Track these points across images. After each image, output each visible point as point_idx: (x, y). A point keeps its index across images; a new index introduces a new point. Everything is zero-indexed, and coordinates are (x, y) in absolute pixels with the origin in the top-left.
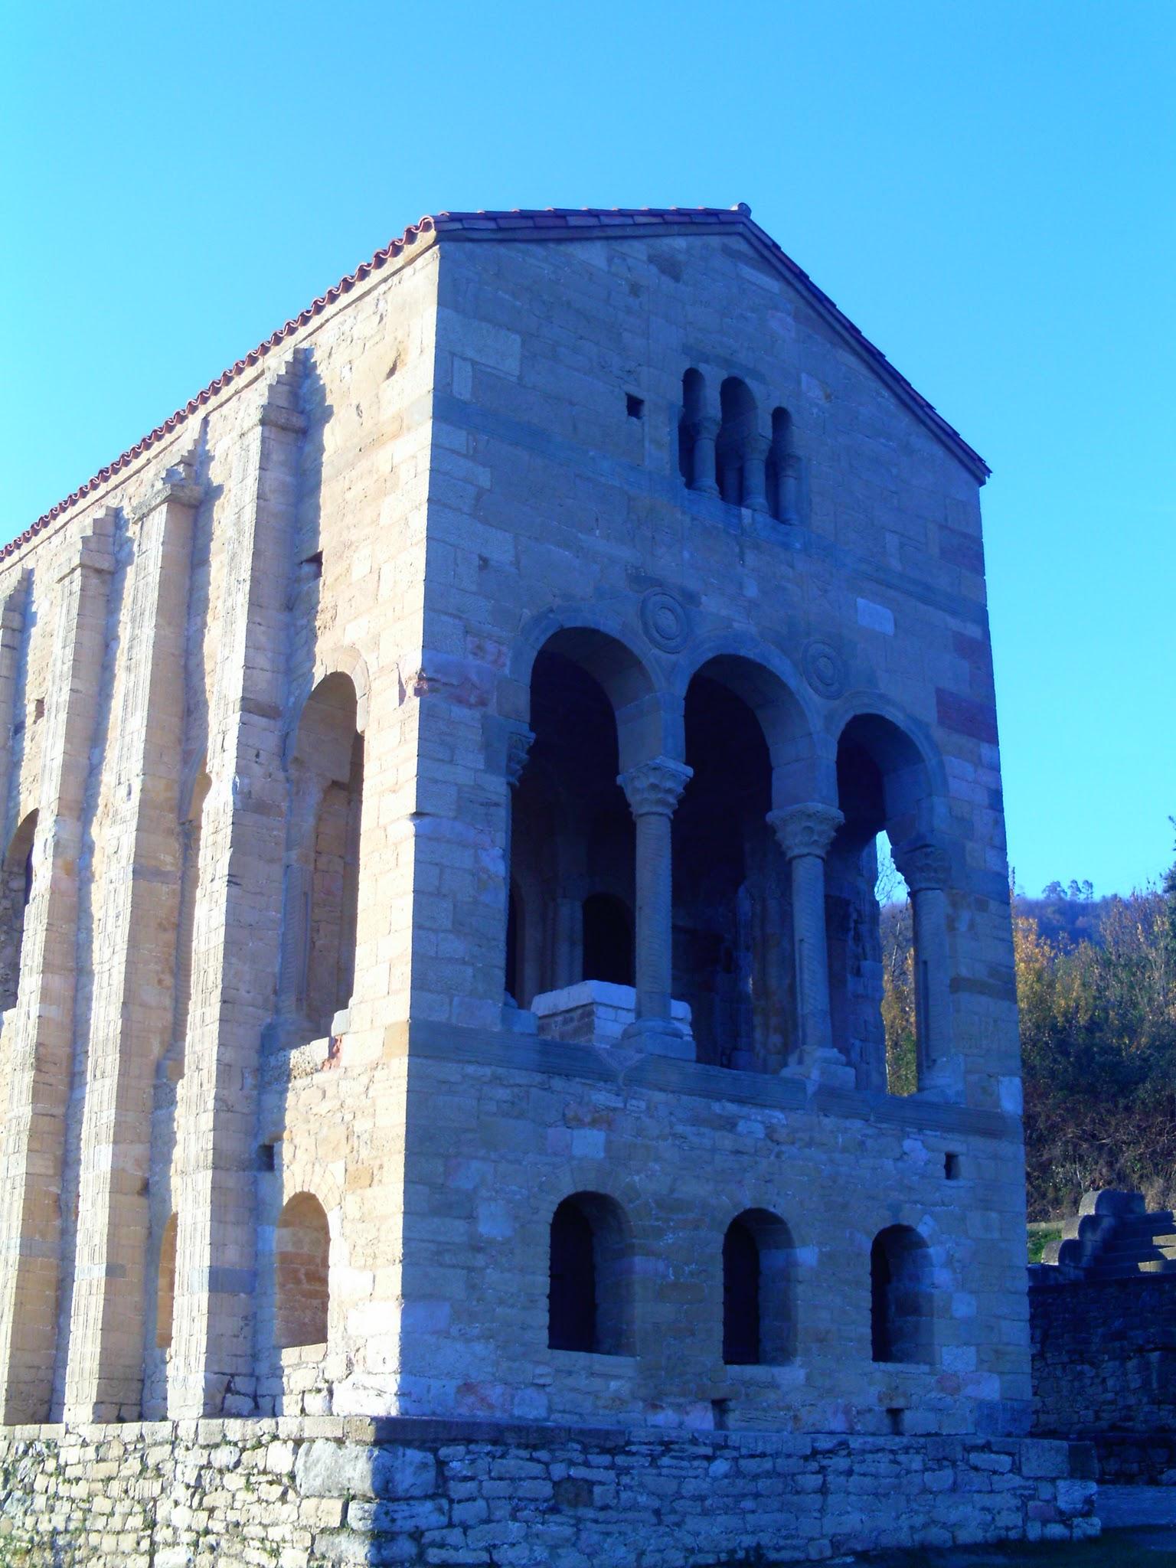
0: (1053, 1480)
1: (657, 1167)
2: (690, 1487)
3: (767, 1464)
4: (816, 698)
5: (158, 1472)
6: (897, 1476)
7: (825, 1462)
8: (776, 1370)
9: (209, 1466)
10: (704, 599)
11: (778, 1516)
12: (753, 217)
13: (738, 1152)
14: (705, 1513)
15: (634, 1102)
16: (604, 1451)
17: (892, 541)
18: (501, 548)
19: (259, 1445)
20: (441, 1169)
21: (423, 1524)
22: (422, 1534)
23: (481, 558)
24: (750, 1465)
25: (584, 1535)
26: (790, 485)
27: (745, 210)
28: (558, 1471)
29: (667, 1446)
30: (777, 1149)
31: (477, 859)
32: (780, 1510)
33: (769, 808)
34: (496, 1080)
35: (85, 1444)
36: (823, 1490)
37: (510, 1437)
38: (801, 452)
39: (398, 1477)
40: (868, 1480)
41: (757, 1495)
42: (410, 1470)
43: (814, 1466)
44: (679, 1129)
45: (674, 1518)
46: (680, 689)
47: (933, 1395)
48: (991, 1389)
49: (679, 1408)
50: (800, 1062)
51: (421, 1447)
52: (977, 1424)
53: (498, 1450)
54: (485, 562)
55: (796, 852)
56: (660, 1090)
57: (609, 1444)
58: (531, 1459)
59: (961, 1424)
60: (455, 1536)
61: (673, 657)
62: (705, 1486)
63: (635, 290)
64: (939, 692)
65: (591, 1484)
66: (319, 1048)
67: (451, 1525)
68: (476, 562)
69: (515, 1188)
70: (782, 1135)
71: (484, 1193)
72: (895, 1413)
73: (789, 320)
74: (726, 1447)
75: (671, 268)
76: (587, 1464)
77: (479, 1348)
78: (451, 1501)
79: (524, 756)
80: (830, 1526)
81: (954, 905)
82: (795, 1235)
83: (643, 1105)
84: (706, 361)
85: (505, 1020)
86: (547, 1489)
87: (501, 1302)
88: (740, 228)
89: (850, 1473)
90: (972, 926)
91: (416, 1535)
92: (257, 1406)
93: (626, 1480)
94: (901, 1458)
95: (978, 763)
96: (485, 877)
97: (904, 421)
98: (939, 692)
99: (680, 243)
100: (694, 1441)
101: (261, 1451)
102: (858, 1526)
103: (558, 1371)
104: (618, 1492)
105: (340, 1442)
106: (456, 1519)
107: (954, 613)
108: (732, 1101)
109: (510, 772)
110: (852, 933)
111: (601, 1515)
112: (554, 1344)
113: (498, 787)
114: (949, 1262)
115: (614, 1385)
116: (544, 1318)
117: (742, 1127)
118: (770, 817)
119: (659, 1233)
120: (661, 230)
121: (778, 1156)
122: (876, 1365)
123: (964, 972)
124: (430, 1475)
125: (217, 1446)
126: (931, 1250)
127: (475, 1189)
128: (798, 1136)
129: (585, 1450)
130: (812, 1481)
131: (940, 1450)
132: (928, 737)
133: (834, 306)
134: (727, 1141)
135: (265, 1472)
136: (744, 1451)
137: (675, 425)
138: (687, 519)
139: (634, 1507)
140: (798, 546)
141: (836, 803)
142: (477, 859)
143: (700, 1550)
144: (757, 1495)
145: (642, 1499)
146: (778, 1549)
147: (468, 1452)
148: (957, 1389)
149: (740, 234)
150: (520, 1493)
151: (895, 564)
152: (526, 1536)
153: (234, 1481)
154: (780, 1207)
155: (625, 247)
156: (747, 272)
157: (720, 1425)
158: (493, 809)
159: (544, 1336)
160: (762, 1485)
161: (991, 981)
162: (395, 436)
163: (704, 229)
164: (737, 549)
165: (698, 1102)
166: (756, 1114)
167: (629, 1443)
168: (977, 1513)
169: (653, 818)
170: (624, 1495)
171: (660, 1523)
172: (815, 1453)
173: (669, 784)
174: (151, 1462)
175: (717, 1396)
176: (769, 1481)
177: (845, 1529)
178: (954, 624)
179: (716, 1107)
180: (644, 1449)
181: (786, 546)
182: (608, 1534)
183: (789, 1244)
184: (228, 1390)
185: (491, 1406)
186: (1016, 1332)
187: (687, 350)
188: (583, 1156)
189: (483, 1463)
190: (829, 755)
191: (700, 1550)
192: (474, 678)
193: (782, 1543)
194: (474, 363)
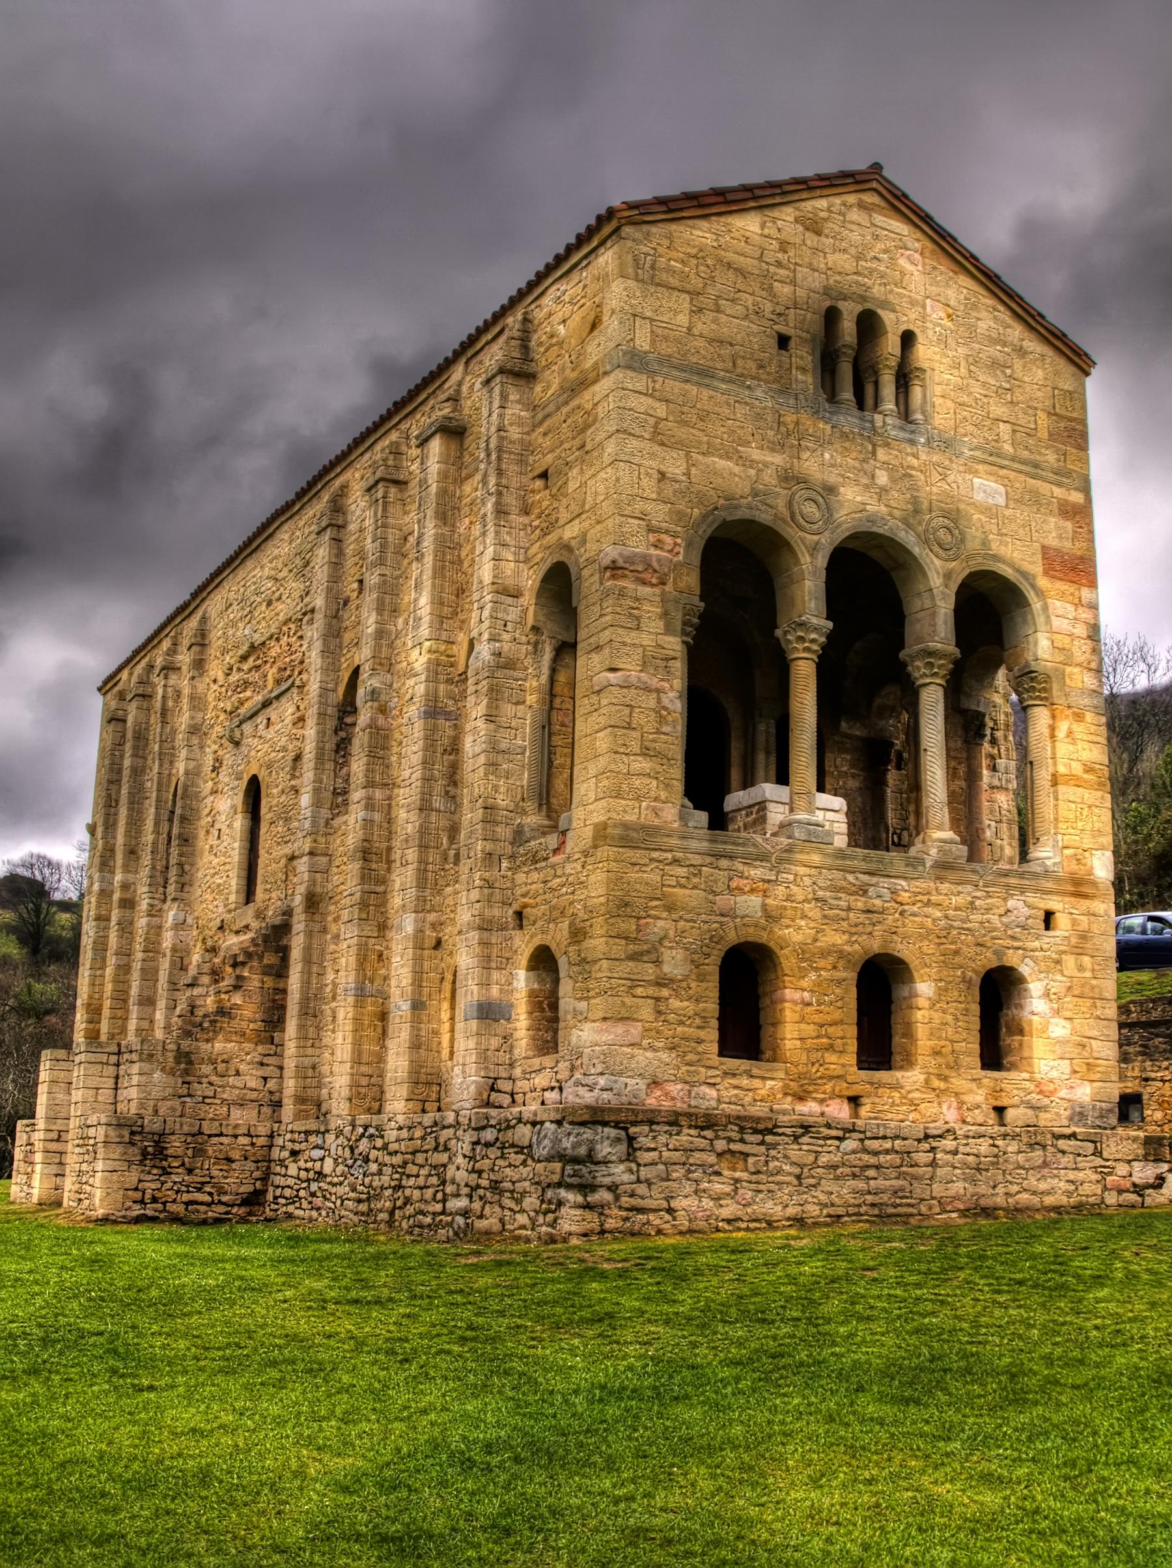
0: (1129, 1162)
1: (803, 923)
2: (824, 1159)
3: (888, 1145)
4: (937, 562)
5: (446, 1149)
6: (996, 1156)
7: (935, 1144)
8: (898, 1074)
9: (477, 1143)
10: (842, 489)
11: (894, 1182)
12: (885, 173)
13: (869, 911)
14: (837, 1178)
16: (756, 1131)
17: (1004, 429)
18: (675, 466)
19: (508, 1127)
21: (617, 1179)
22: (617, 1187)
23: (659, 472)
24: (874, 1145)
25: (741, 1191)
26: (917, 393)
27: (877, 167)
28: (720, 1145)
29: (806, 1128)
31: (659, 701)
32: (897, 1178)
33: (901, 645)
35: (400, 1128)
36: (933, 1164)
37: (684, 1121)
38: (925, 365)
39: (598, 1147)
40: (971, 1158)
41: (877, 1167)
42: (606, 1143)
44: (820, 893)
45: (812, 1181)
46: (822, 561)
48: (1084, 1093)
49: (822, 1101)
50: (924, 842)
51: (616, 1127)
52: (1071, 1119)
53: (675, 1129)
54: (662, 475)
55: (922, 681)
57: (761, 1126)
58: (699, 1136)
59: (1056, 1117)
60: (642, 1189)
61: (816, 538)
62: (836, 1158)
63: (784, 246)
64: (1045, 549)
65: (747, 1155)
66: (552, 841)
67: (639, 1181)
68: (656, 476)
70: (905, 896)
71: (667, 944)
72: (1000, 1110)
73: (917, 256)
74: (854, 1131)
75: (814, 226)
76: (742, 1141)
77: (664, 1056)
78: (639, 1165)
79: (696, 620)
80: (938, 1189)
81: (1054, 717)
82: (915, 974)
83: (791, 877)
84: (845, 299)
85: (682, 818)
86: (712, 1159)
87: (681, 1023)
88: (874, 185)
89: (955, 1153)
90: (1070, 733)
91: (613, 1188)
92: (514, 1101)
93: (773, 1153)
94: (999, 1143)
95: (1079, 604)
96: (664, 713)
97: (1016, 332)
98: (1045, 549)
99: (823, 203)
100: (828, 1126)
101: (510, 1133)
102: (962, 1191)
103: (725, 1073)
105: (559, 1123)
106: (642, 1178)
107: (1059, 485)
109: (684, 633)
110: (988, 738)
111: (754, 1178)
112: (721, 1054)
113: (674, 645)
114: (1047, 994)
115: (769, 1083)
116: (715, 1035)
117: (872, 891)
118: (902, 655)
120: (805, 195)
121: (901, 914)
122: (984, 1073)
123: (1062, 769)
124: (622, 1148)
125: (484, 1128)
126: (1031, 986)
129: (742, 1130)
130: (923, 1158)
131: (1034, 1137)
132: (1033, 586)
133: (955, 240)
135: (513, 1146)
136: (868, 1134)
137: (818, 354)
138: (828, 427)
139: (779, 1172)
140: (922, 440)
141: (954, 642)
142: (659, 701)
143: (833, 1205)
144: (877, 1167)
145: (787, 1168)
146: (895, 1206)
147: (652, 1131)
148: (1052, 1093)
149: (875, 190)
150: (691, 1161)
151: (1008, 448)
152: (696, 1192)
153: (493, 1153)
154: (903, 950)
155: (775, 213)
156: (879, 219)
157: (856, 1115)
159: (715, 1048)
160: (882, 1158)
161: (1085, 776)
162: (595, 381)
163: (840, 190)
164: (870, 448)
166: (885, 882)
167: (775, 1126)
168: (1062, 1184)
169: (801, 662)
170: (771, 1165)
171: (800, 1185)
172: (927, 1136)
173: (813, 636)
174: (442, 1140)
175: (850, 1093)
176: (888, 1157)
177: (951, 1193)
178: (1058, 492)
179: (851, 878)
180: (788, 1131)
181: (912, 442)
182: (760, 1191)
183: (911, 980)
184: (492, 1089)
185: (673, 1099)
186: (1106, 1050)
187: (827, 291)
189: (662, 1139)
190: (945, 607)
191: (833, 1205)
192: (655, 565)
193: (898, 1201)
194: (652, 320)
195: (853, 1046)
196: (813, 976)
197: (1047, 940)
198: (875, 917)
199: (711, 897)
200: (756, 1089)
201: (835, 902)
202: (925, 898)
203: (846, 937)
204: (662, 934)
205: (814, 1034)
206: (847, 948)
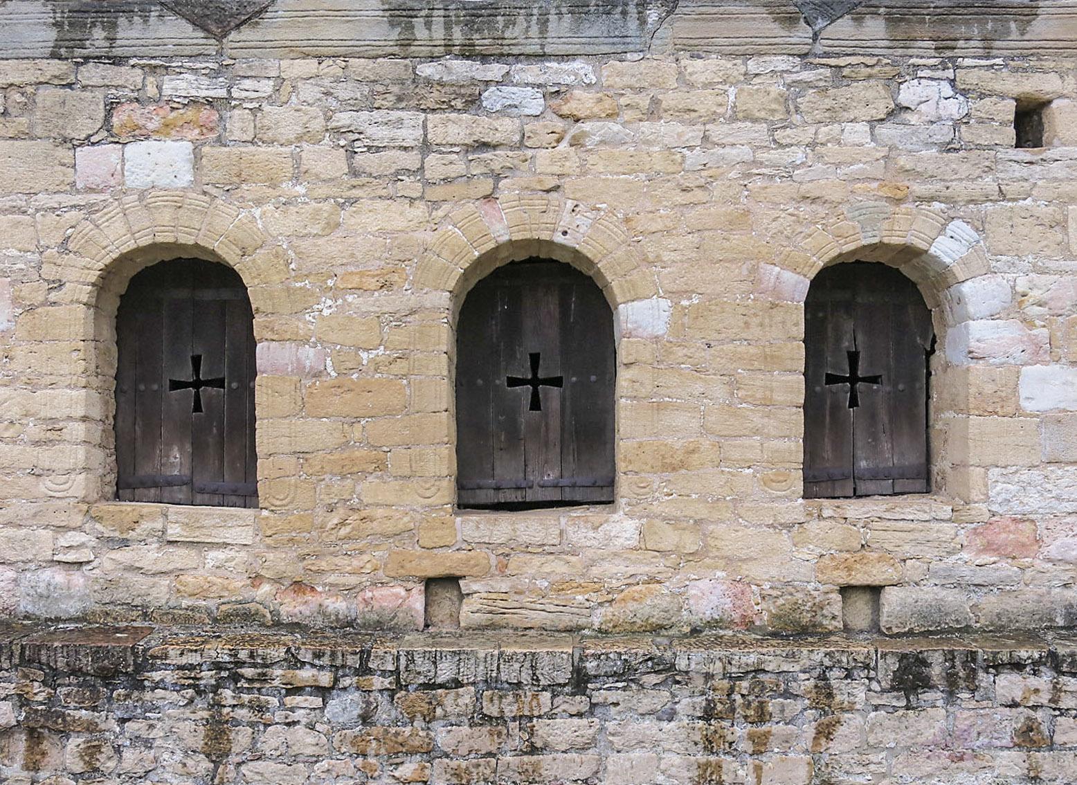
1: (300, 189)
15: (247, 84)
30: (575, 129)
43: (580, 703)
44: (343, 119)
47: (965, 555)
56: (306, 56)
69: (16, 253)
70: (582, 101)
83: (267, 87)
104: (118, 750)
117: (491, 98)
119: (302, 303)
121: (576, 142)
126: (966, 288)
128: (623, 101)
134: (455, 128)
154: (575, 230)
166: (530, 72)
195: (440, 460)
196: (327, 307)
197: (1019, 171)
198: (497, 159)
199: (63, 153)
200: (197, 556)
201: (381, 134)
202: (644, 101)
203: (420, 210)
205: (337, 439)
206: (429, 237)
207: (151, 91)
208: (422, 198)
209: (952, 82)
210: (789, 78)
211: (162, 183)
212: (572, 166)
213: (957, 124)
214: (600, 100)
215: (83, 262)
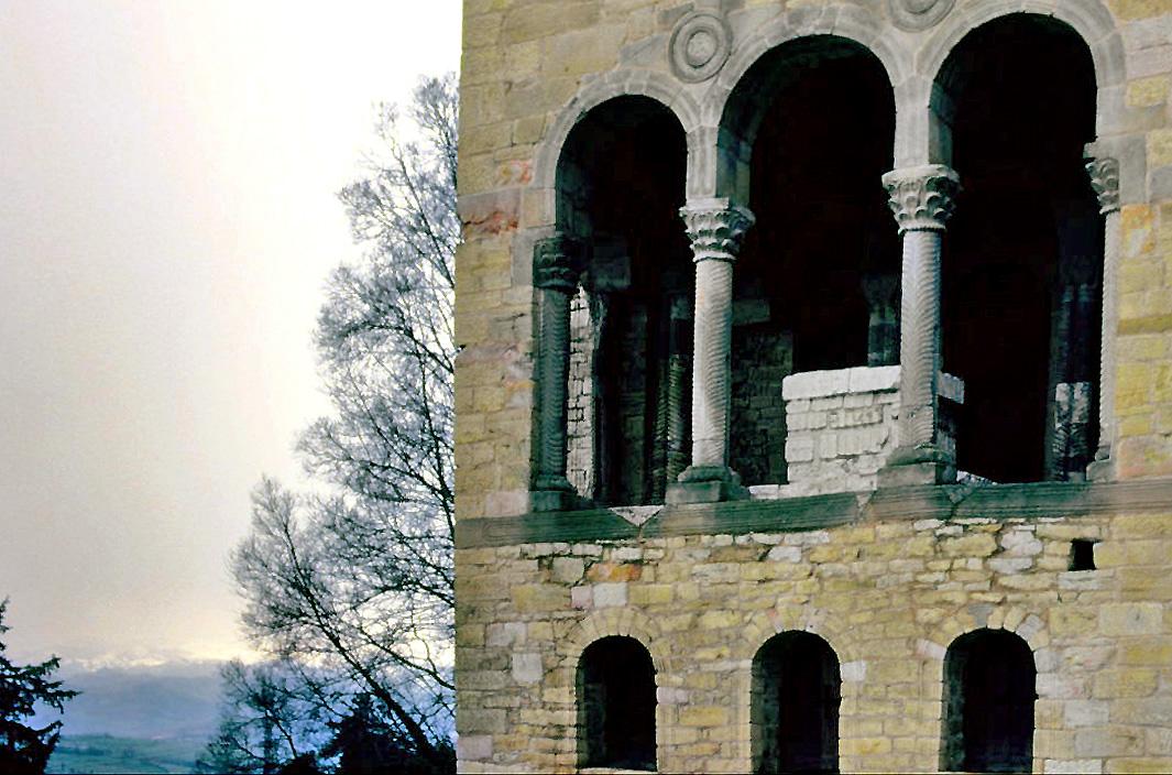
20: (482, 634)
34: (524, 556)
44: (698, 568)
108: (764, 531)
117: (773, 554)
121: (819, 577)
127: (510, 646)
134: (756, 571)
158: (519, 320)
165: (723, 540)
166: (796, 538)
179: (741, 540)
188: (609, 608)
199: (565, 590)
203: (737, 616)
204: (510, 639)
207: (606, 557)
208: (738, 609)
209: (1034, 532)
210: (938, 532)
211: (612, 604)
212: (816, 588)
213: (1035, 557)
214: (831, 552)
215: (574, 646)
